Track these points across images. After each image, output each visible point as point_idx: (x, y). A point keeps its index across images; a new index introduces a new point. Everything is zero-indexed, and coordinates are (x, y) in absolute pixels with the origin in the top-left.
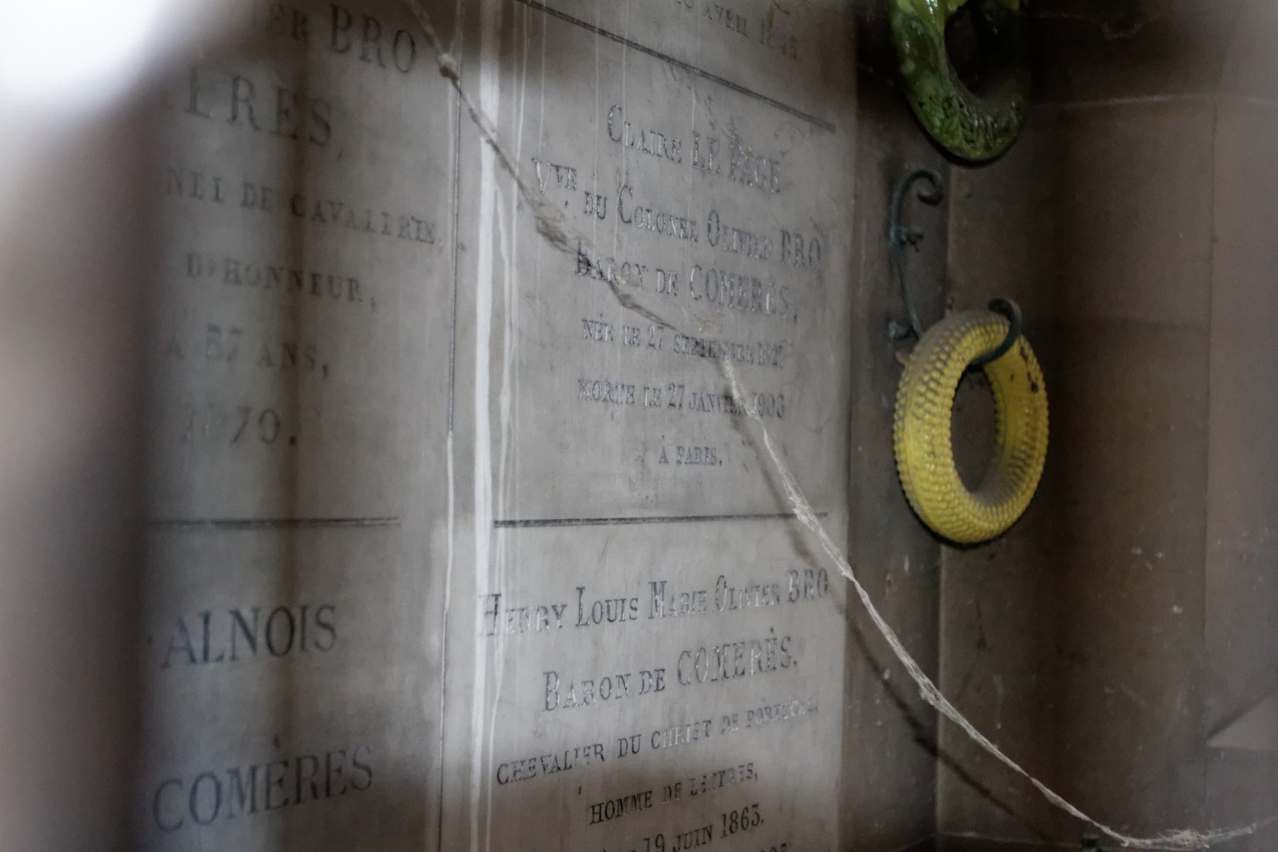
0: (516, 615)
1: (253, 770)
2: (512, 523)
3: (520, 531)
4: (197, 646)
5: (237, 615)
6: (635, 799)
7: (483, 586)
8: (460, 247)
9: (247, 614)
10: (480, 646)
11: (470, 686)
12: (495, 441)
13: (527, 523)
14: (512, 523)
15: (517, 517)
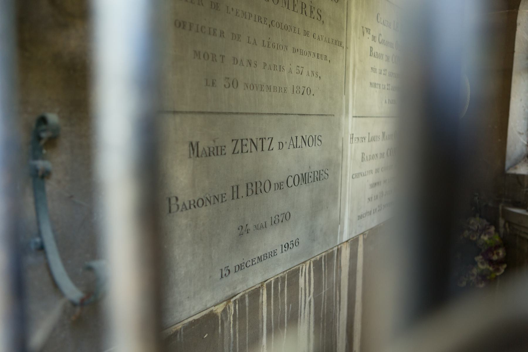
0: (357, 139)
1: (305, 174)
2: (356, 117)
3: (358, 119)
4: (295, 144)
5: (303, 137)
6: (378, 183)
7: (350, 132)
8: (347, 48)
9: (304, 137)
10: (349, 145)
11: (347, 156)
12: (353, 96)
13: (359, 117)
14: (356, 117)
15: (357, 115)
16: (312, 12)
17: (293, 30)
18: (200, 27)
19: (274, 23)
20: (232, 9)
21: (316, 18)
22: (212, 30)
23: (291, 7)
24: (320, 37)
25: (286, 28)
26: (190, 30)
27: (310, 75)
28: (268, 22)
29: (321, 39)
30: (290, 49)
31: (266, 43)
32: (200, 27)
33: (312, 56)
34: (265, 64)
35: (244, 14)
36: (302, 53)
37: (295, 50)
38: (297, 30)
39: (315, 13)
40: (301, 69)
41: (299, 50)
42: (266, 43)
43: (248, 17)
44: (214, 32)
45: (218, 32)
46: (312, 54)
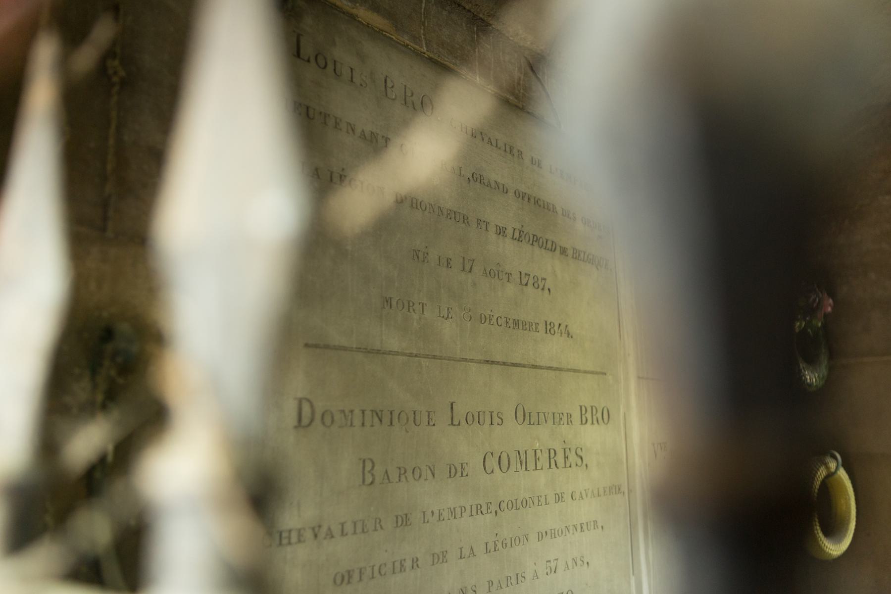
16: (566, 458)
17: (536, 501)
18: (376, 569)
19: (504, 505)
20: (433, 512)
21: (573, 465)
22: (397, 565)
23: (531, 465)
24: (584, 493)
25: (525, 504)
26: (361, 579)
27: (570, 567)
28: (494, 508)
29: (584, 496)
30: (533, 537)
31: (491, 546)
32: (376, 569)
33: (571, 532)
34: (491, 583)
35: (452, 512)
36: (553, 534)
37: (541, 536)
38: (543, 500)
39: (573, 458)
40: (553, 565)
41: (549, 533)
42: (491, 546)
43: (458, 515)
44: (402, 565)
45: (408, 564)
46: (571, 528)
